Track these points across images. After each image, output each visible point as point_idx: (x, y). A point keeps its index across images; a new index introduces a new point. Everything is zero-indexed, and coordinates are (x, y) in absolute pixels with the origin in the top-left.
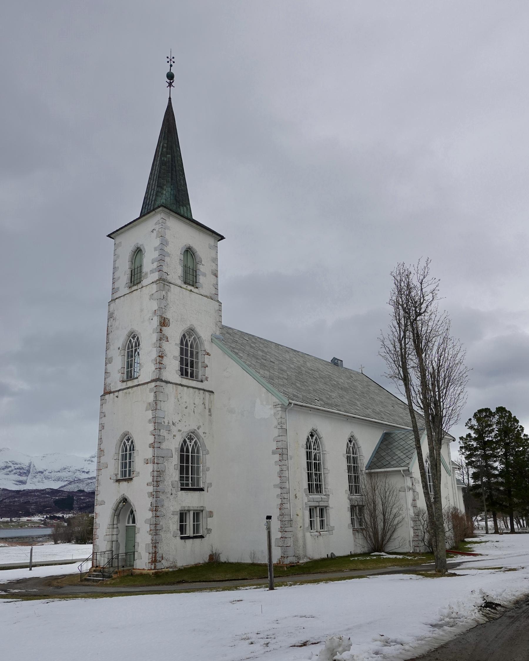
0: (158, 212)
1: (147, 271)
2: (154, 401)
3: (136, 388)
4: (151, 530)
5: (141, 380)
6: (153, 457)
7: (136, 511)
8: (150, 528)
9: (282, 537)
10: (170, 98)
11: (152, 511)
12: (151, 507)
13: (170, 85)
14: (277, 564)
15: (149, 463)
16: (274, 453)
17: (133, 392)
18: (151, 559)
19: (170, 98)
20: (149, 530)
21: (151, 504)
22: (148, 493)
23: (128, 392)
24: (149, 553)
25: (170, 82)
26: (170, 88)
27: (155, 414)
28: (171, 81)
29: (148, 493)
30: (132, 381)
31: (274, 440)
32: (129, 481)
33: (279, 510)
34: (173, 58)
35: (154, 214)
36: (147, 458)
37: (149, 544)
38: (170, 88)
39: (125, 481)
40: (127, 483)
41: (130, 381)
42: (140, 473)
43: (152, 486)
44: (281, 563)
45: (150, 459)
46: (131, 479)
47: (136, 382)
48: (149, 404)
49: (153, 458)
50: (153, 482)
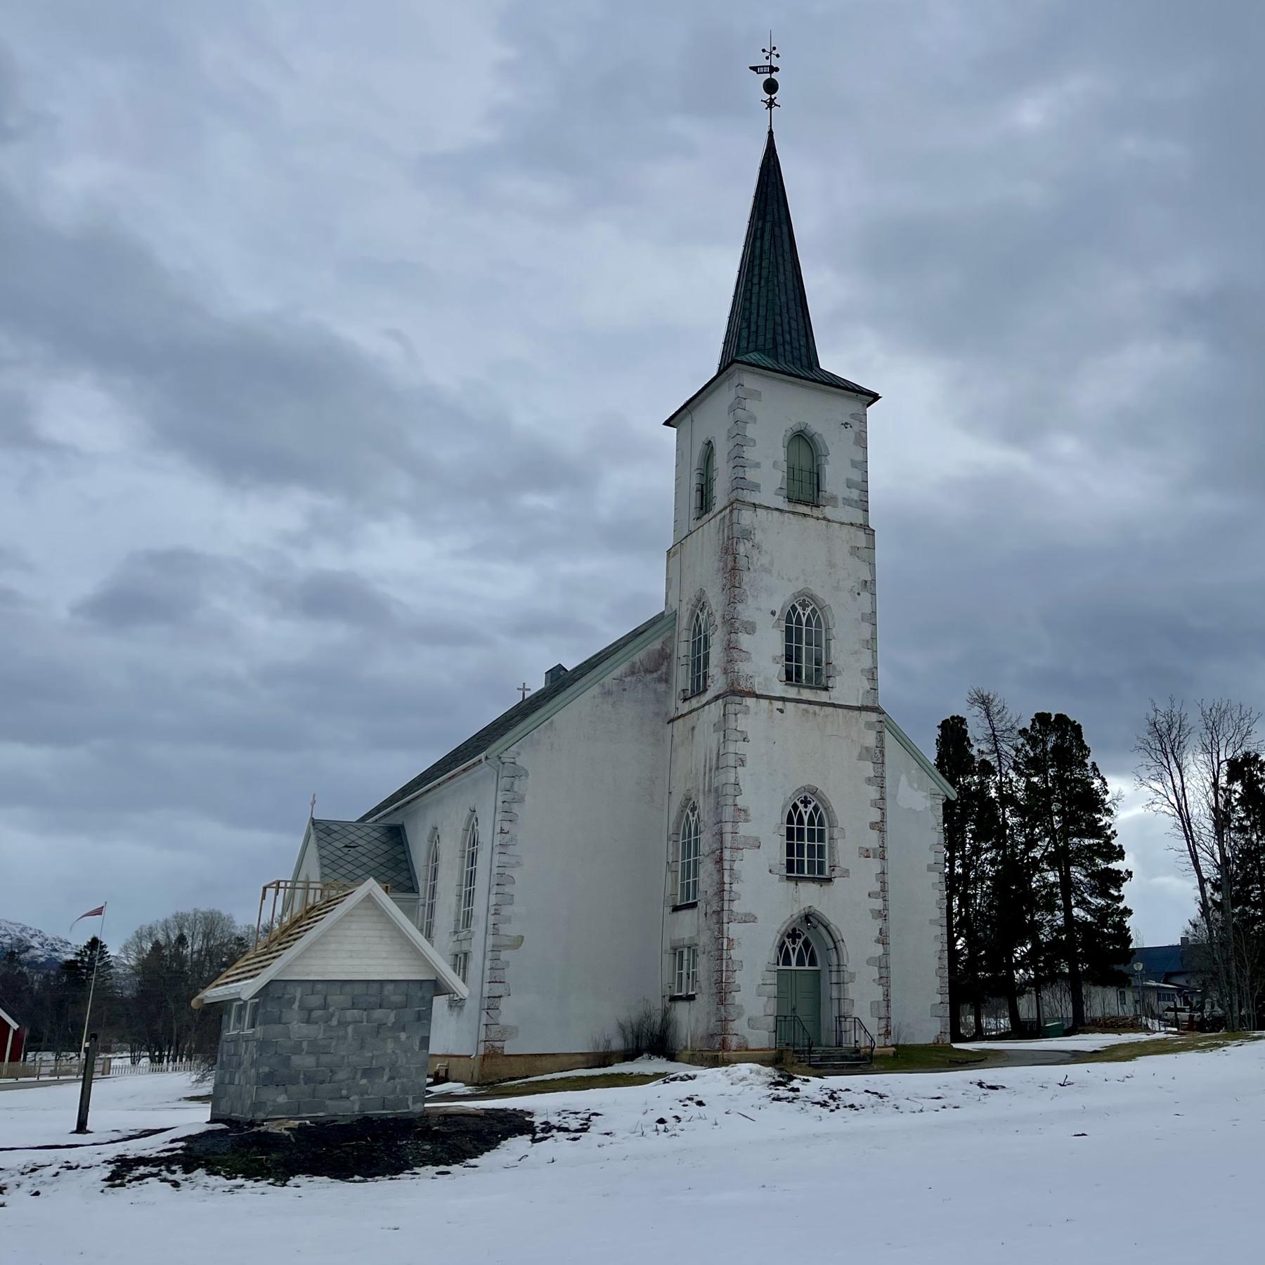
0: (861, 400)
1: (834, 494)
2: (877, 747)
3: (831, 709)
4: (881, 978)
5: (835, 696)
6: (881, 847)
7: (843, 941)
8: (880, 973)
9: (942, 1003)
10: (771, 133)
11: (883, 944)
12: (880, 936)
13: (771, 104)
14: (934, 1043)
15: (871, 855)
16: (930, 869)
17: (827, 716)
18: (885, 1029)
19: (771, 133)
20: (878, 977)
21: (880, 932)
22: (872, 911)
23: (811, 711)
24: (880, 1018)
25: (771, 98)
26: (771, 110)
27: (880, 771)
28: (773, 96)
29: (872, 911)
30: (815, 691)
31: (931, 849)
32: (823, 883)
33: (937, 959)
34: (774, 48)
35: (851, 397)
36: (867, 846)
37: (878, 1002)
38: (771, 110)
39: (813, 882)
40: (819, 886)
41: (808, 690)
42: (851, 871)
43: (881, 900)
44: (941, 1042)
45: (874, 849)
46: (829, 880)
47: (823, 696)
48: (867, 749)
49: (882, 849)
50: (881, 893)
